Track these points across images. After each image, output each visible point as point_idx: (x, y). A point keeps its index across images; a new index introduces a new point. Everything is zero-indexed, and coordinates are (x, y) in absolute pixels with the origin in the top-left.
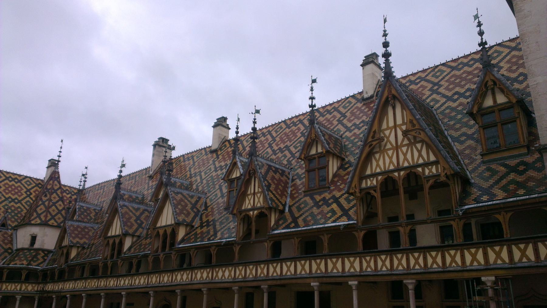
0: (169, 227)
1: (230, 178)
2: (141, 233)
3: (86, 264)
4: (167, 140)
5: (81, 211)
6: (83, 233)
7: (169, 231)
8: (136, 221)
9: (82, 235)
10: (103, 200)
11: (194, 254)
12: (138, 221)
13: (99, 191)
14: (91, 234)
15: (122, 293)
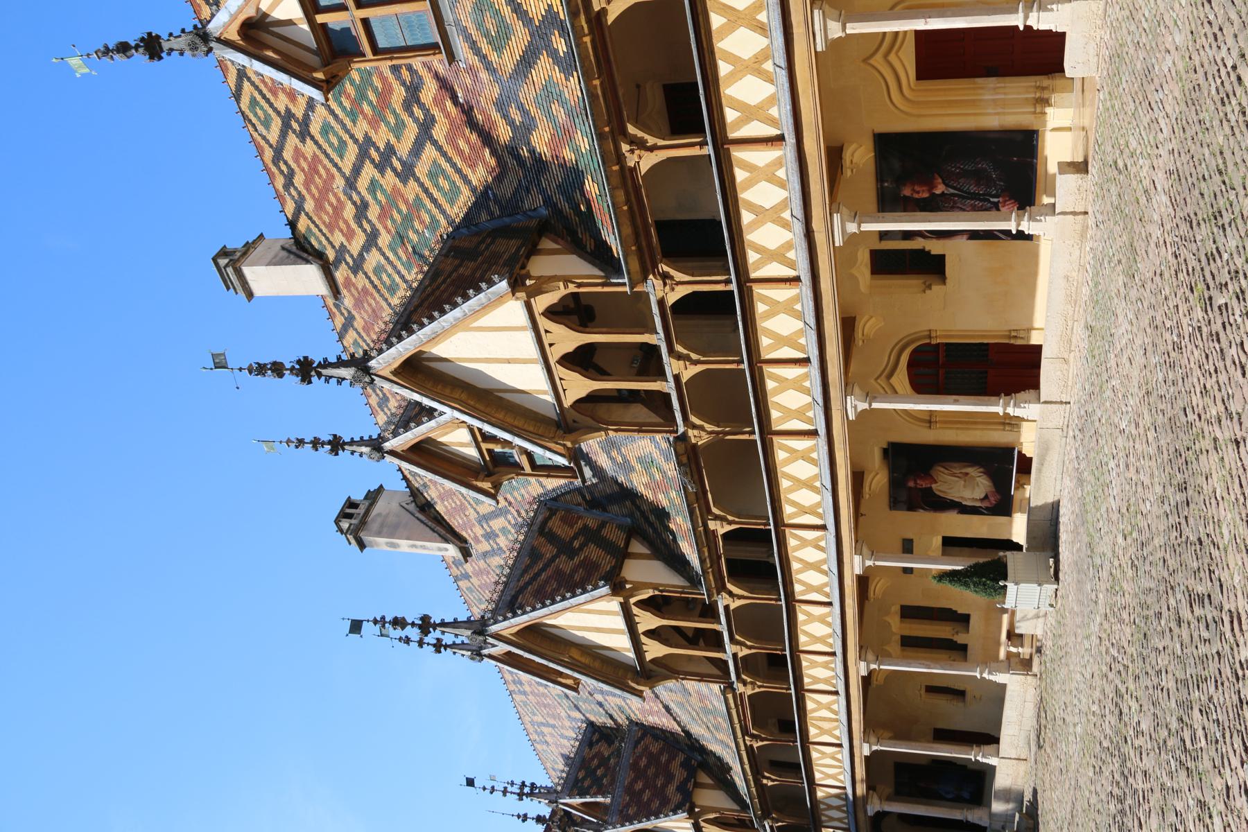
0: (546, 340)
1: (314, 60)
2: (620, 527)
3: (750, 750)
4: (351, 504)
5: (590, 787)
6: (651, 771)
7: (566, 339)
8: (572, 553)
9: (656, 776)
10: (567, 723)
11: (651, 140)
12: (576, 544)
13: (548, 739)
14: (655, 747)
15: (858, 570)
